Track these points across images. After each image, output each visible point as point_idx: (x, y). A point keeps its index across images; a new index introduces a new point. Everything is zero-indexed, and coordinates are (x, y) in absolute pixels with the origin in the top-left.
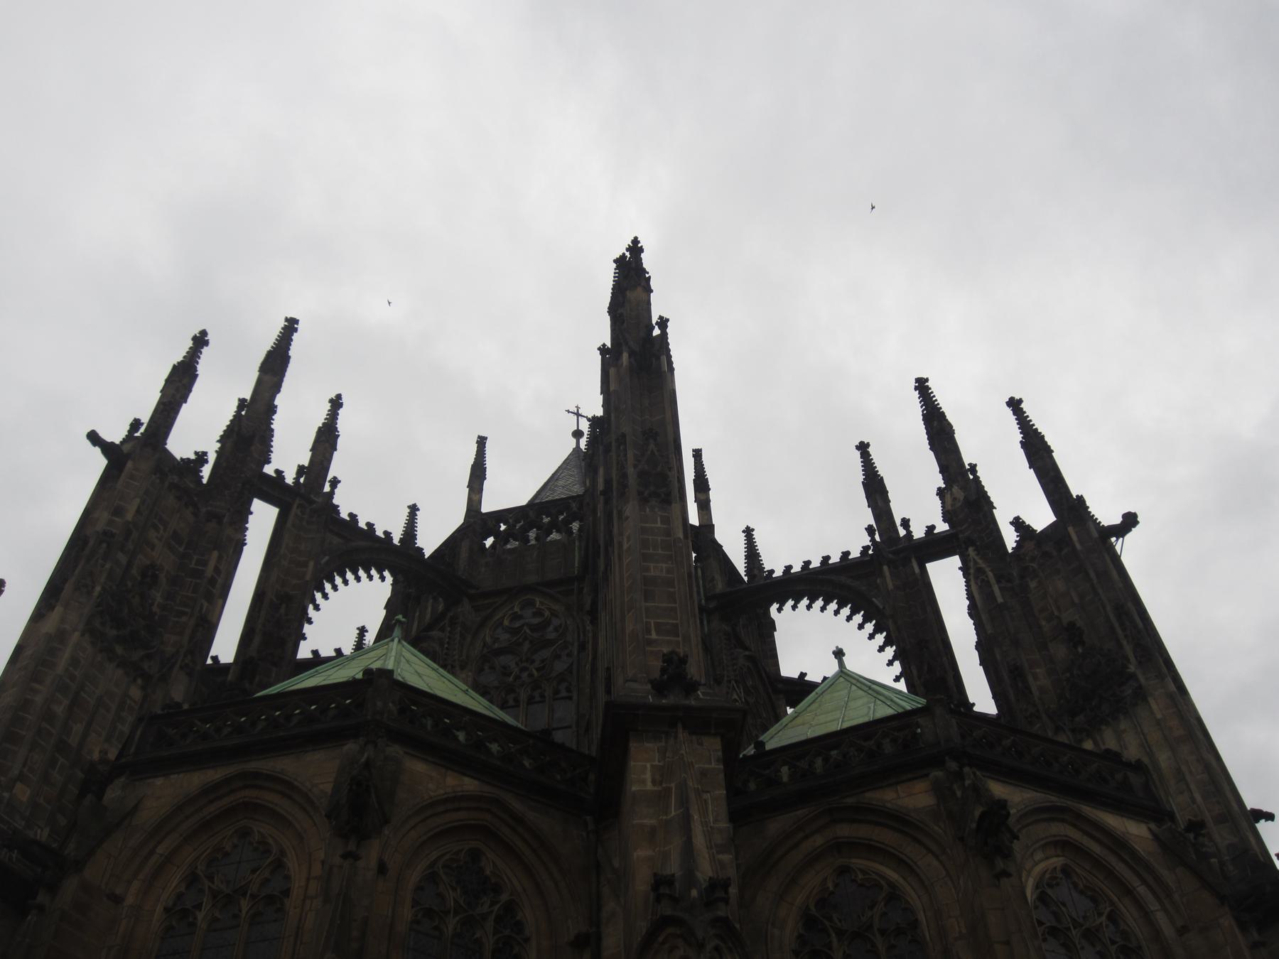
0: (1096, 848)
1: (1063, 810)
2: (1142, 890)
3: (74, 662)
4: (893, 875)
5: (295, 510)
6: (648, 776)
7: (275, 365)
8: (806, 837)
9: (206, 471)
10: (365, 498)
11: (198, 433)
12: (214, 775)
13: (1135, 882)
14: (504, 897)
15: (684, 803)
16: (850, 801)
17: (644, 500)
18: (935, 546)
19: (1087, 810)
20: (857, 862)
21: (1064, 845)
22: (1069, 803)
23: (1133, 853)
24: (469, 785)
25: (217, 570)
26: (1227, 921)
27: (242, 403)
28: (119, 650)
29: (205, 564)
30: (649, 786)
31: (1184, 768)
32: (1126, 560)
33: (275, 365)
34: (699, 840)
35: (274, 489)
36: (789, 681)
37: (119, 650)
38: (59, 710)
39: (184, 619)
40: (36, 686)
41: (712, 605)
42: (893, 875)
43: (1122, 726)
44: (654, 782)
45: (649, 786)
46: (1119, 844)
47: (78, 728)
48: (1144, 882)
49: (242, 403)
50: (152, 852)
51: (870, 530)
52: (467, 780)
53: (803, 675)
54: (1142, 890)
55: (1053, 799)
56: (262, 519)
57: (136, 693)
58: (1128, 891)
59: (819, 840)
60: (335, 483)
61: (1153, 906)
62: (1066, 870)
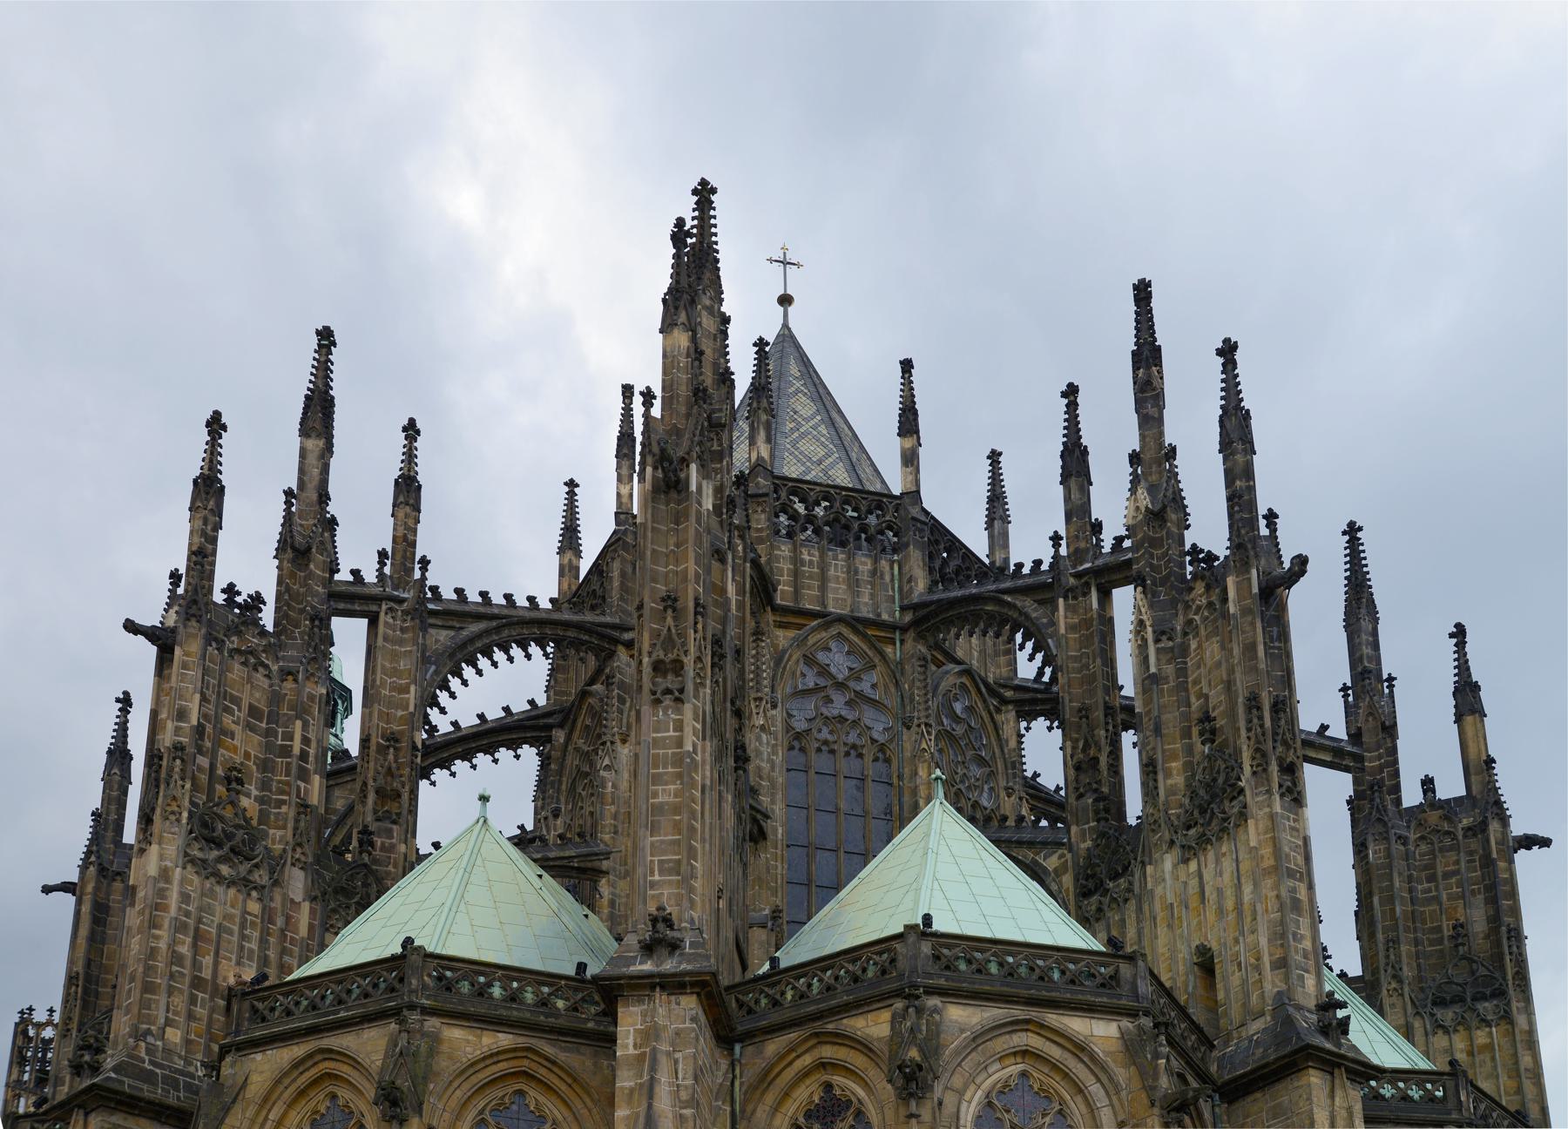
0: (1055, 1052)
1: (1027, 1021)
2: (1095, 1089)
3: (185, 898)
4: (861, 1093)
6: (631, 1041)
16: (830, 1027)
19: (1053, 1018)
20: (838, 1079)
21: (1025, 1053)
23: (1093, 1057)
24: (505, 1040)
25: (306, 741)
29: (289, 736)
31: (1259, 907)
41: (908, 618)
42: (861, 1093)
43: (1224, 849)
44: (635, 1046)
45: (631, 1051)
46: (1079, 1048)
54: (1095, 1089)
55: (1018, 1012)
58: (1079, 1090)
59: (807, 1060)
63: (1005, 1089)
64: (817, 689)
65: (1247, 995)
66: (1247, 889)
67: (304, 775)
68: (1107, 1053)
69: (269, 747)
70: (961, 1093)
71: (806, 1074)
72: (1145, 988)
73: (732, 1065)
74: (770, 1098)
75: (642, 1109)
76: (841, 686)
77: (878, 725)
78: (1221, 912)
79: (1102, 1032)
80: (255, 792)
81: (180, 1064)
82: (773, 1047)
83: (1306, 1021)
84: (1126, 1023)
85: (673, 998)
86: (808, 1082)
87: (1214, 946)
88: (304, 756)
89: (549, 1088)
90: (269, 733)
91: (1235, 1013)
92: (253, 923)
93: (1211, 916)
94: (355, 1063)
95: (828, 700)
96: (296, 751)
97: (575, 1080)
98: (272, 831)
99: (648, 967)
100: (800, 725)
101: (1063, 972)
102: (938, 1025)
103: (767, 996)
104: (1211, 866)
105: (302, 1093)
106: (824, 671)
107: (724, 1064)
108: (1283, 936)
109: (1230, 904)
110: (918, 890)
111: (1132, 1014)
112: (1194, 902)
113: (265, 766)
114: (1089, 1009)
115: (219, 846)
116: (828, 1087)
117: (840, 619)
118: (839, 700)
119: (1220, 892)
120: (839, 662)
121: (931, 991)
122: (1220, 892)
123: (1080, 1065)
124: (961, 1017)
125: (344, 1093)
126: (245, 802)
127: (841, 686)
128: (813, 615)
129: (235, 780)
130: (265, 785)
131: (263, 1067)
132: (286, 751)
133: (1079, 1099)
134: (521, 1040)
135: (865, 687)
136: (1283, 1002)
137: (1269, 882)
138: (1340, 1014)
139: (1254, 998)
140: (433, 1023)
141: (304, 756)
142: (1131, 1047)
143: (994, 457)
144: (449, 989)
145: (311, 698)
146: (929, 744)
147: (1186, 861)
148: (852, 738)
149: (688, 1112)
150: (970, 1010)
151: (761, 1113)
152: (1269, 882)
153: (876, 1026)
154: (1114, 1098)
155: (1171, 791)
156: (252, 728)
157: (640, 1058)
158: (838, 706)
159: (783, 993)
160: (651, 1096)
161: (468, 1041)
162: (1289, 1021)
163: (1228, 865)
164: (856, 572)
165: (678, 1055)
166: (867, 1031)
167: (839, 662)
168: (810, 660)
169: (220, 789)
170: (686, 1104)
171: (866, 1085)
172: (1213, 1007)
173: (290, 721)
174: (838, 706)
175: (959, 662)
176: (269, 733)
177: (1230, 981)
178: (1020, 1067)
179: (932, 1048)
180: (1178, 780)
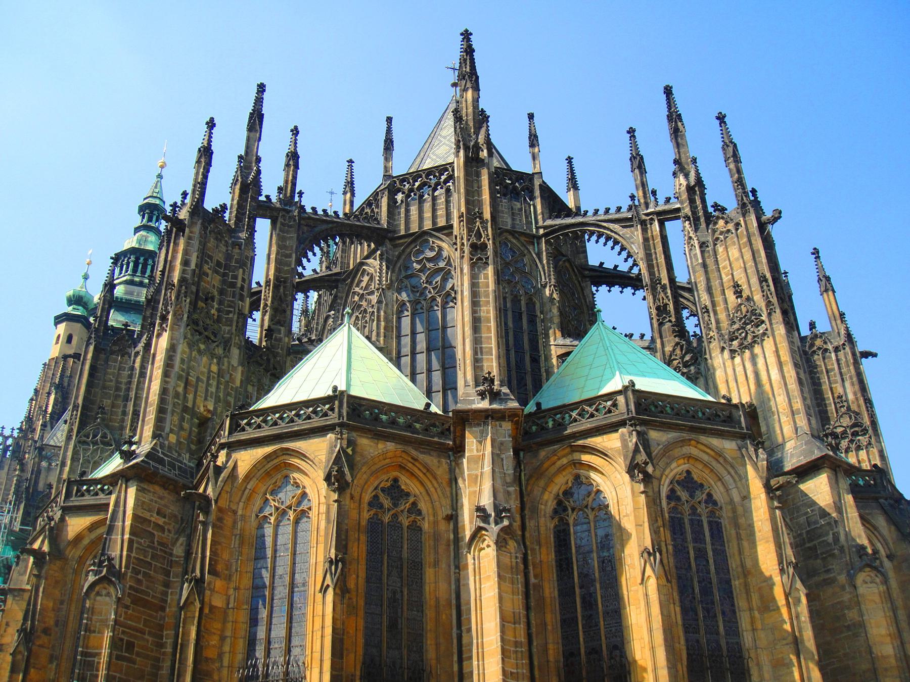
2: (728, 478)
3: (182, 361)
5: (280, 220)
7: (256, 119)
8: (559, 459)
10: (321, 195)
11: (220, 194)
13: (724, 473)
14: (412, 499)
16: (580, 442)
19: (703, 438)
21: (689, 457)
22: (693, 436)
23: (725, 459)
24: (390, 446)
25: (243, 280)
27: (240, 157)
29: (236, 277)
30: (475, 453)
32: (773, 235)
33: (256, 119)
35: (266, 209)
36: (593, 269)
37: (202, 347)
39: (231, 315)
40: (167, 379)
45: (475, 453)
46: (719, 455)
47: (190, 397)
48: (729, 473)
49: (240, 157)
50: (246, 488)
52: (388, 443)
53: (602, 264)
55: (685, 435)
56: (263, 226)
57: (214, 368)
59: (565, 461)
60: (301, 194)
62: (688, 472)
67: (242, 298)
68: (733, 458)
69: (224, 282)
71: (563, 468)
80: (216, 306)
85: (497, 423)
86: (564, 473)
88: (242, 288)
90: (224, 275)
92: (214, 377)
96: (239, 285)
97: (428, 470)
98: (223, 328)
101: (704, 414)
102: (648, 440)
103: (537, 425)
113: (222, 292)
114: (721, 434)
115: (200, 334)
117: (507, 231)
123: (719, 465)
129: (208, 298)
130: (221, 303)
132: (233, 285)
133: (719, 484)
134: (399, 446)
141: (242, 288)
144: (359, 416)
145: (247, 257)
149: (511, 489)
150: (661, 433)
154: (739, 484)
156: (217, 272)
159: (547, 423)
161: (371, 446)
164: (512, 209)
165: (503, 456)
166: (604, 444)
173: (237, 268)
175: (564, 256)
176: (224, 275)
178: (686, 467)
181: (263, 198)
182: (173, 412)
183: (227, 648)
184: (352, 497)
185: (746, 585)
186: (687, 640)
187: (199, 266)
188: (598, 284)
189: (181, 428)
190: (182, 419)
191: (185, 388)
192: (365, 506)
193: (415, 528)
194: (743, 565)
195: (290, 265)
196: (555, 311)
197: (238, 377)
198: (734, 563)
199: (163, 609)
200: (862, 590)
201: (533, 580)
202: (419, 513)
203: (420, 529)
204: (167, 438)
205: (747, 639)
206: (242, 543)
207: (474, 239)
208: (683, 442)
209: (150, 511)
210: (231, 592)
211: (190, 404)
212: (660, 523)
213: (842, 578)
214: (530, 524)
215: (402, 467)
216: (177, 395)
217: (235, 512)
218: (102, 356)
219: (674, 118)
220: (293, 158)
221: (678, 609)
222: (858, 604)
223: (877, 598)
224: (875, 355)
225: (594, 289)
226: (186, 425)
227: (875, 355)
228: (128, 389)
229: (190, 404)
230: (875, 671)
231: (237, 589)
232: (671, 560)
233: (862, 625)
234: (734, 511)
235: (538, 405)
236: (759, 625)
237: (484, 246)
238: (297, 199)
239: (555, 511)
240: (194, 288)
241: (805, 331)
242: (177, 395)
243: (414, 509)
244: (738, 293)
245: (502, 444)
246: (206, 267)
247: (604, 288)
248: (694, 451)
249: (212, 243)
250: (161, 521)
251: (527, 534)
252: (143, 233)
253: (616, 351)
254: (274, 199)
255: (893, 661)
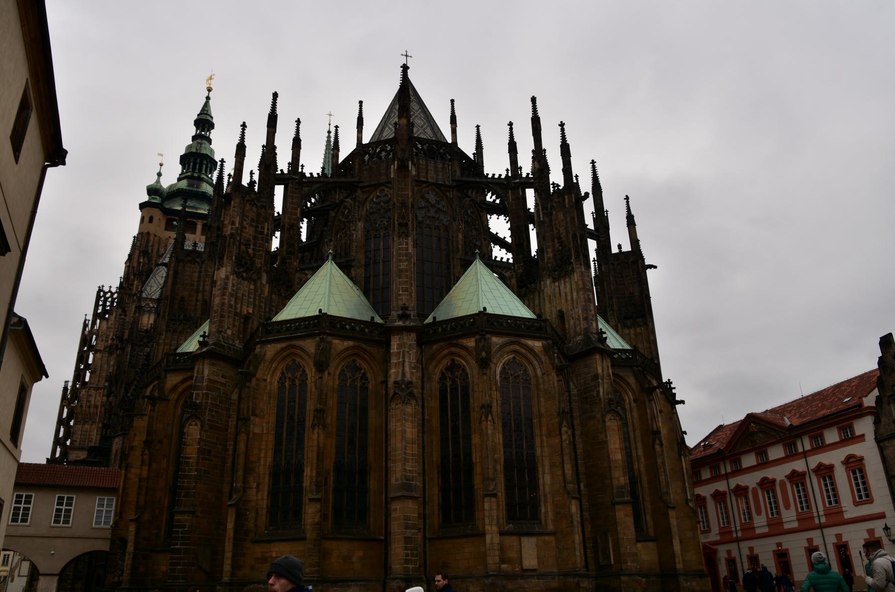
0: (523, 351)
2: (535, 362)
5: (290, 185)
9: (256, 188)
12: (283, 345)
15: (404, 357)
17: (400, 236)
18: (527, 183)
19: (523, 341)
21: (514, 351)
22: (517, 339)
23: (535, 352)
24: (351, 343)
26: (554, 374)
27: (263, 146)
28: (244, 275)
34: (407, 369)
35: (281, 179)
37: (244, 275)
38: (232, 303)
41: (454, 184)
46: (531, 350)
47: (239, 306)
49: (263, 146)
51: (507, 170)
54: (535, 362)
55: (513, 339)
57: (252, 287)
58: (531, 363)
59: (447, 351)
60: (302, 166)
61: (537, 366)
62: (514, 358)
63: (507, 363)
64: (425, 207)
65: (575, 328)
66: (575, 294)
69: (256, 232)
70: (496, 365)
71: (446, 356)
72: (549, 330)
73: (422, 352)
74: (434, 363)
75: (400, 370)
76: (433, 206)
77: (445, 219)
78: (566, 300)
79: (537, 345)
81: (231, 342)
82: (435, 347)
83: (594, 337)
84: (544, 342)
87: (564, 310)
89: (363, 359)
90: (256, 227)
91: (572, 331)
93: (563, 301)
94: (303, 350)
95: (429, 211)
99: (401, 323)
100: (420, 219)
104: (563, 285)
105: (284, 359)
106: (427, 201)
107: (419, 351)
108: (586, 310)
109: (569, 298)
110: (478, 295)
111: (546, 339)
112: (558, 296)
113: (255, 238)
116: (453, 360)
117: (433, 184)
118: (432, 210)
119: (566, 294)
120: (432, 198)
121: (488, 332)
122: (566, 294)
124: (496, 340)
125: (298, 360)
126: (250, 251)
127: (433, 206)
128: (425, 182)
129: (247, 245)
130: (255, 245)
131: (271, 350)
132: (262, 233)
135: (440, 206)
136: (587, 331)
137: (581, 293)
138: (604, 336)
139: (578, 328)
140: (330, 339)
142: (546, 349)
143: (478, 127)
146: (462, 226)
147: (554, 282)
148: (436, 224)
151: (431, 368)
152: (581, 293)
153: (471, 343)
155: (549, 258)
156: (251, 225)
157: (399, 353)
158: (432, 213)
160: (403, 366)
162: (589, 338)
163: (568, 285)
167: (432, 198)
168: (423, 197)
169: (243, 247)
170: (414, 368)
171: (466, 361)
172: (564, 329)
174: (432, 213)
176: (256, 227)
177: (570, 323)
178: (511, 356)
179: (489, 353)
180: (551, 255)
181: (279, 172)
182: (229, 317)
183: (262, 455)
184: (329, 374)
185: (540, 422)
186: (505, 452)
187: (241, 223)
188: (492, 214)
189: (234, 325)
190: (234, 320)
191: (235, 302)
192: (337, 377)
193: (364, 388)
194: (539, 411)
195: (296, 214)
196: (460, 236)
197: (266, 290)
198: (535, 410)
199: (227, 430)
200: (608, 424)
201: (427, 417)
202: (367, 379)
203: (367, 388)
204: (226, 333)
205: (538, 451)
206: (270, 397)
207: (401, 221)
208: (512, 343)
209: (218, 376)
210: (264, 424)
211: (238, 311)
212: (494, 388)
213: (599, 416)
214: (427, 385)
215: (356, 355)
216: (230, 306)
217: (266, 380)
218: (181, 264)
219: (536, 122)
220: (297, 144)
221: (501, 436)
222: (606, 431)
223: (616, 428)
224: (655, 267)
225: (489, 216)
226: (237, 323)
227: (655, 267)
228: (198, 286)
229: (238, 311)
230: (610, 467)
231: (268, 423)
232: (499, 409)
233: (606, 442)
234: (537, 381)
235: (434, 318)
236: (545, 444)
237: (406, 225)
238: (300, 170)
239: (441, 379)
240: (238, 238)
241: (615, 250)
242: (230, 306)
243: (364, 377)
244: (561, 243)
245: (410, 345)
246: (245, 223)
247: (495, 216)
248: (517, 348)
249: (248, 207)
250: (224, 381)
251: (425, 392)
252: (199, 141)
253: (483, 282)
254: (286, 172)
255: (620, 462)
